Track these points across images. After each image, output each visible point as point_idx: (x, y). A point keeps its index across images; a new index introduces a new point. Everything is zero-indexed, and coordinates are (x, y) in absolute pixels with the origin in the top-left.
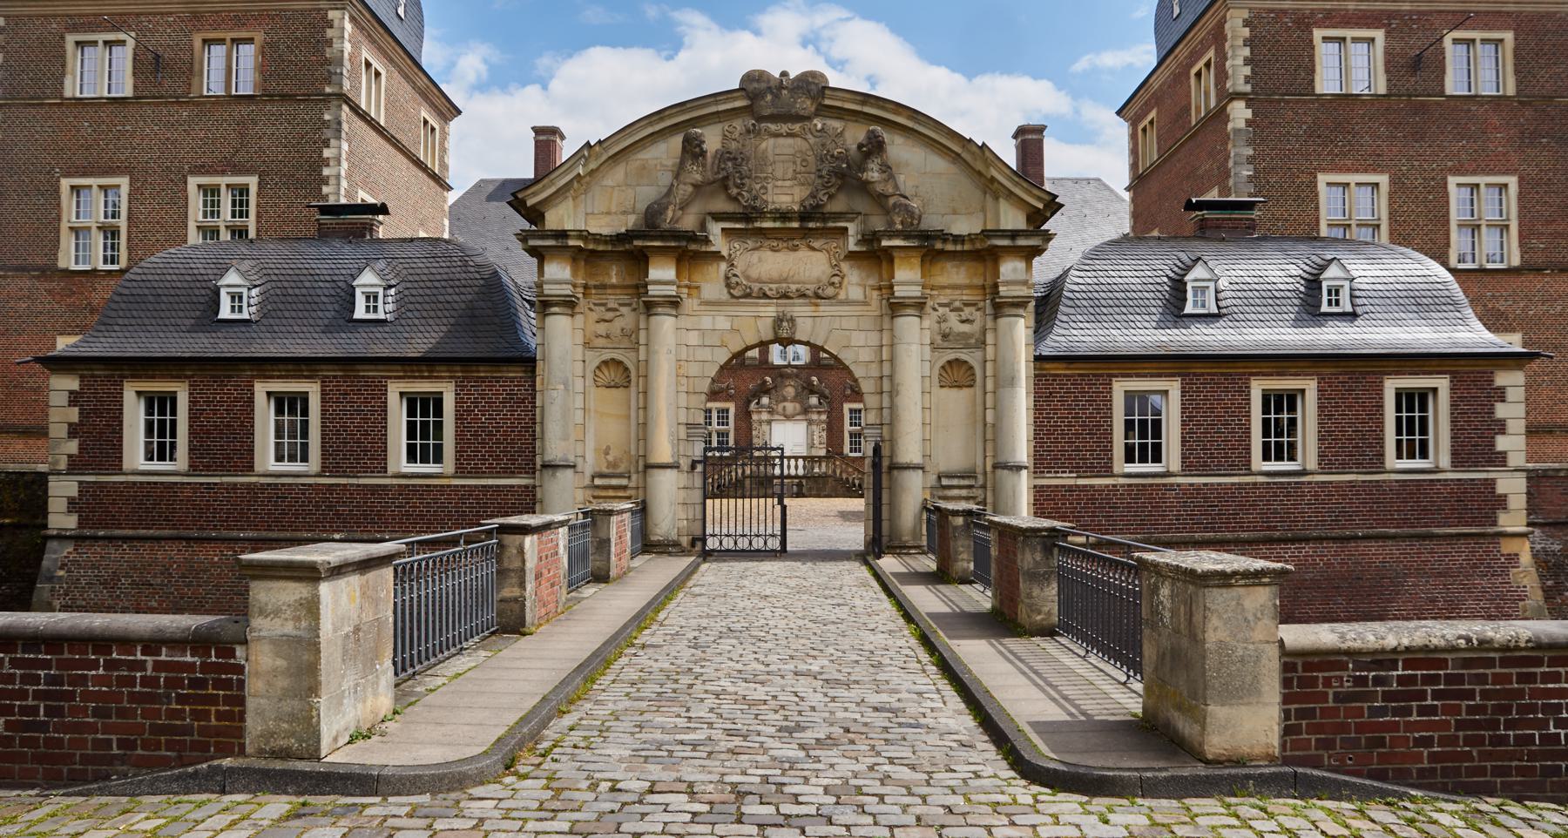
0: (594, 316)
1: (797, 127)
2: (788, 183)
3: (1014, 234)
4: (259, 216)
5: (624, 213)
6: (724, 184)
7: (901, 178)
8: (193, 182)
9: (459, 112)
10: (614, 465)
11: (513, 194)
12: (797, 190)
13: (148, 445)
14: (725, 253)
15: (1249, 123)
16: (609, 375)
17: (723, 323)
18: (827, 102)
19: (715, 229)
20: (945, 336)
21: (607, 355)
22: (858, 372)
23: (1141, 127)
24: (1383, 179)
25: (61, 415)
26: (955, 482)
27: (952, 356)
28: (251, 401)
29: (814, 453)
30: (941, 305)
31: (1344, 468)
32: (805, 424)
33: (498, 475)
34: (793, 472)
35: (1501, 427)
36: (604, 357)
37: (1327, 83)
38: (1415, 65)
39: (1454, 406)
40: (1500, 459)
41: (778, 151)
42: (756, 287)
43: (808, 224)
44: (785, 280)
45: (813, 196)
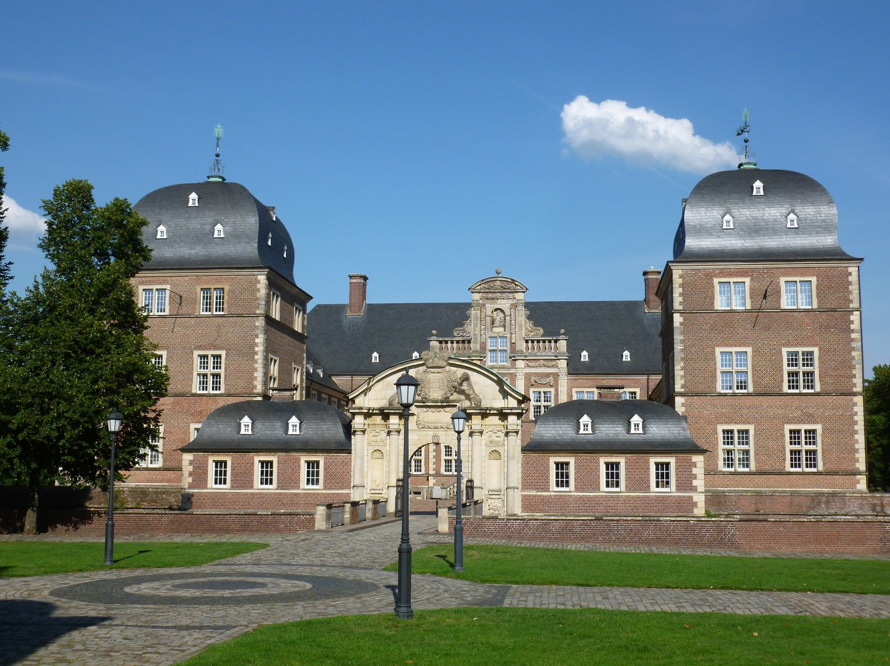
0: (372, 434)
1: (440, 370)
3: (512, 409)
4: (226, 369)
7: (475, 388)
8: (196, 353)
9: (312, 298)
13: (216, 479)
15: (681, 324)
16: (377, 454)
24: (749, 350)
25: (187, 468)
28: (253, 464)
31: (635, 491)
33: (338, 489)
35: (695, 477)
37: (720, 304)
38: (766, 295)
39: (677, 469)
40: (694, 489)
43: (445, 403)
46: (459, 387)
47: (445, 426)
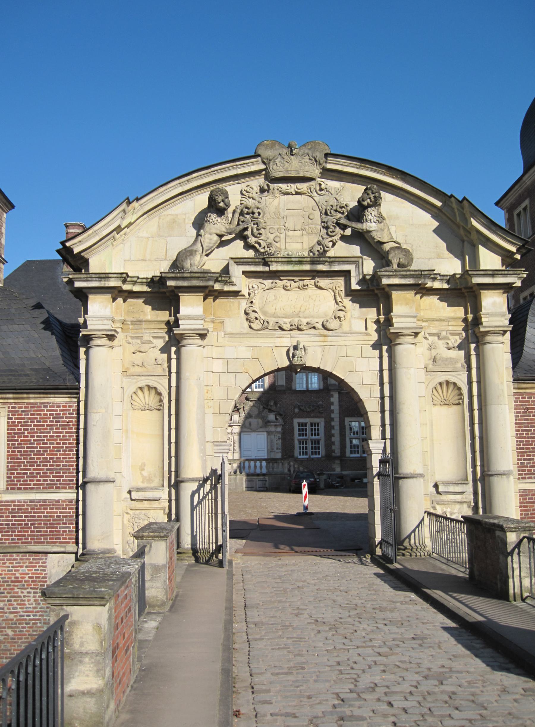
1: (303, 187)
2: (298, 233)
3: (494, 273)
5: (157, 260)
6: (241, 236)
10: (150, 480)
11: (63, 243)
12: (305, 239)
14: (245, 292)
17: (244, 352)
18: (329, 166)
19: (236, 271)
20: (435, 360)
21: (143, 382)
22: (363, 394)
23: (515, 213)
26: (451, 489)
27: (442, 378)
29: (273, 456)
30: (431, 334)
32: (265, 433)
34: (258, 471)
36: (142, 384)
41: (288, 207)
42: (272, 321)
44: (298, 315)
45: (319, 243)
46: (353, 223)
47: (318, 322)
